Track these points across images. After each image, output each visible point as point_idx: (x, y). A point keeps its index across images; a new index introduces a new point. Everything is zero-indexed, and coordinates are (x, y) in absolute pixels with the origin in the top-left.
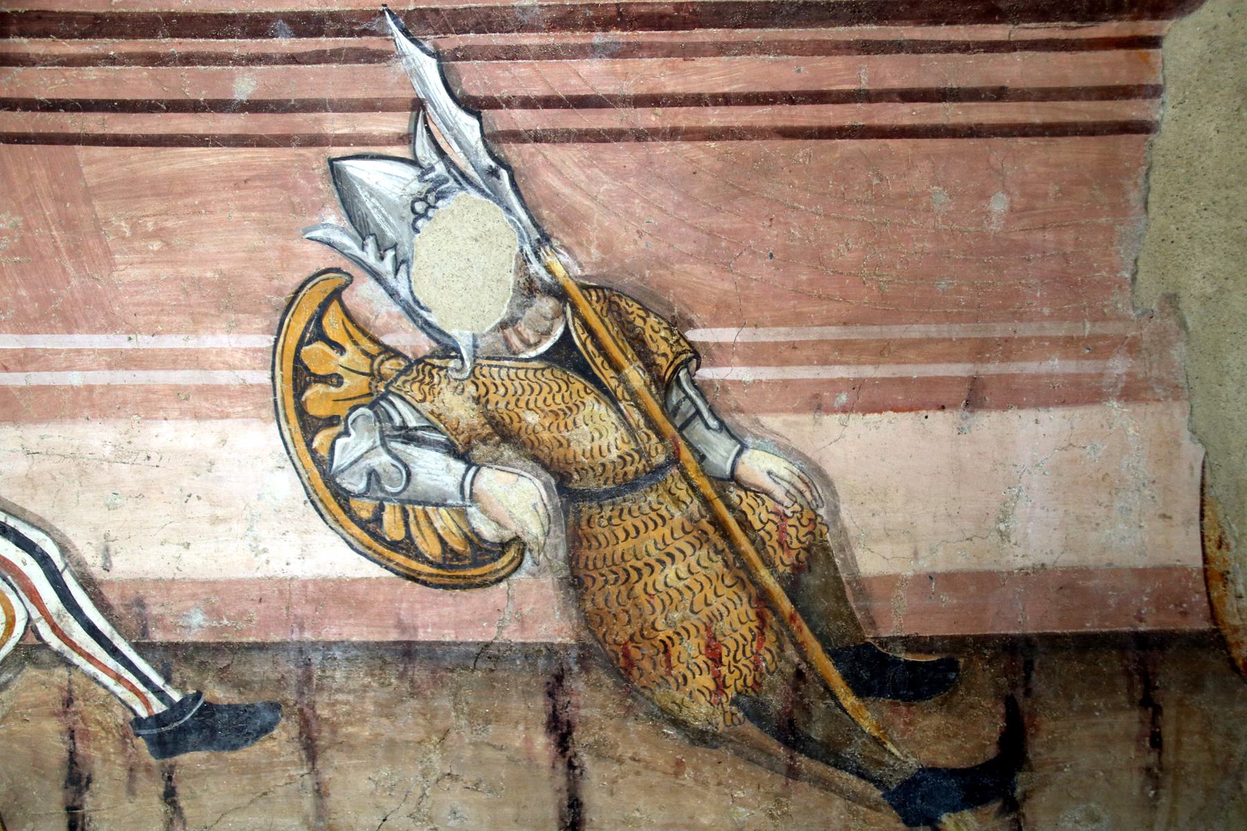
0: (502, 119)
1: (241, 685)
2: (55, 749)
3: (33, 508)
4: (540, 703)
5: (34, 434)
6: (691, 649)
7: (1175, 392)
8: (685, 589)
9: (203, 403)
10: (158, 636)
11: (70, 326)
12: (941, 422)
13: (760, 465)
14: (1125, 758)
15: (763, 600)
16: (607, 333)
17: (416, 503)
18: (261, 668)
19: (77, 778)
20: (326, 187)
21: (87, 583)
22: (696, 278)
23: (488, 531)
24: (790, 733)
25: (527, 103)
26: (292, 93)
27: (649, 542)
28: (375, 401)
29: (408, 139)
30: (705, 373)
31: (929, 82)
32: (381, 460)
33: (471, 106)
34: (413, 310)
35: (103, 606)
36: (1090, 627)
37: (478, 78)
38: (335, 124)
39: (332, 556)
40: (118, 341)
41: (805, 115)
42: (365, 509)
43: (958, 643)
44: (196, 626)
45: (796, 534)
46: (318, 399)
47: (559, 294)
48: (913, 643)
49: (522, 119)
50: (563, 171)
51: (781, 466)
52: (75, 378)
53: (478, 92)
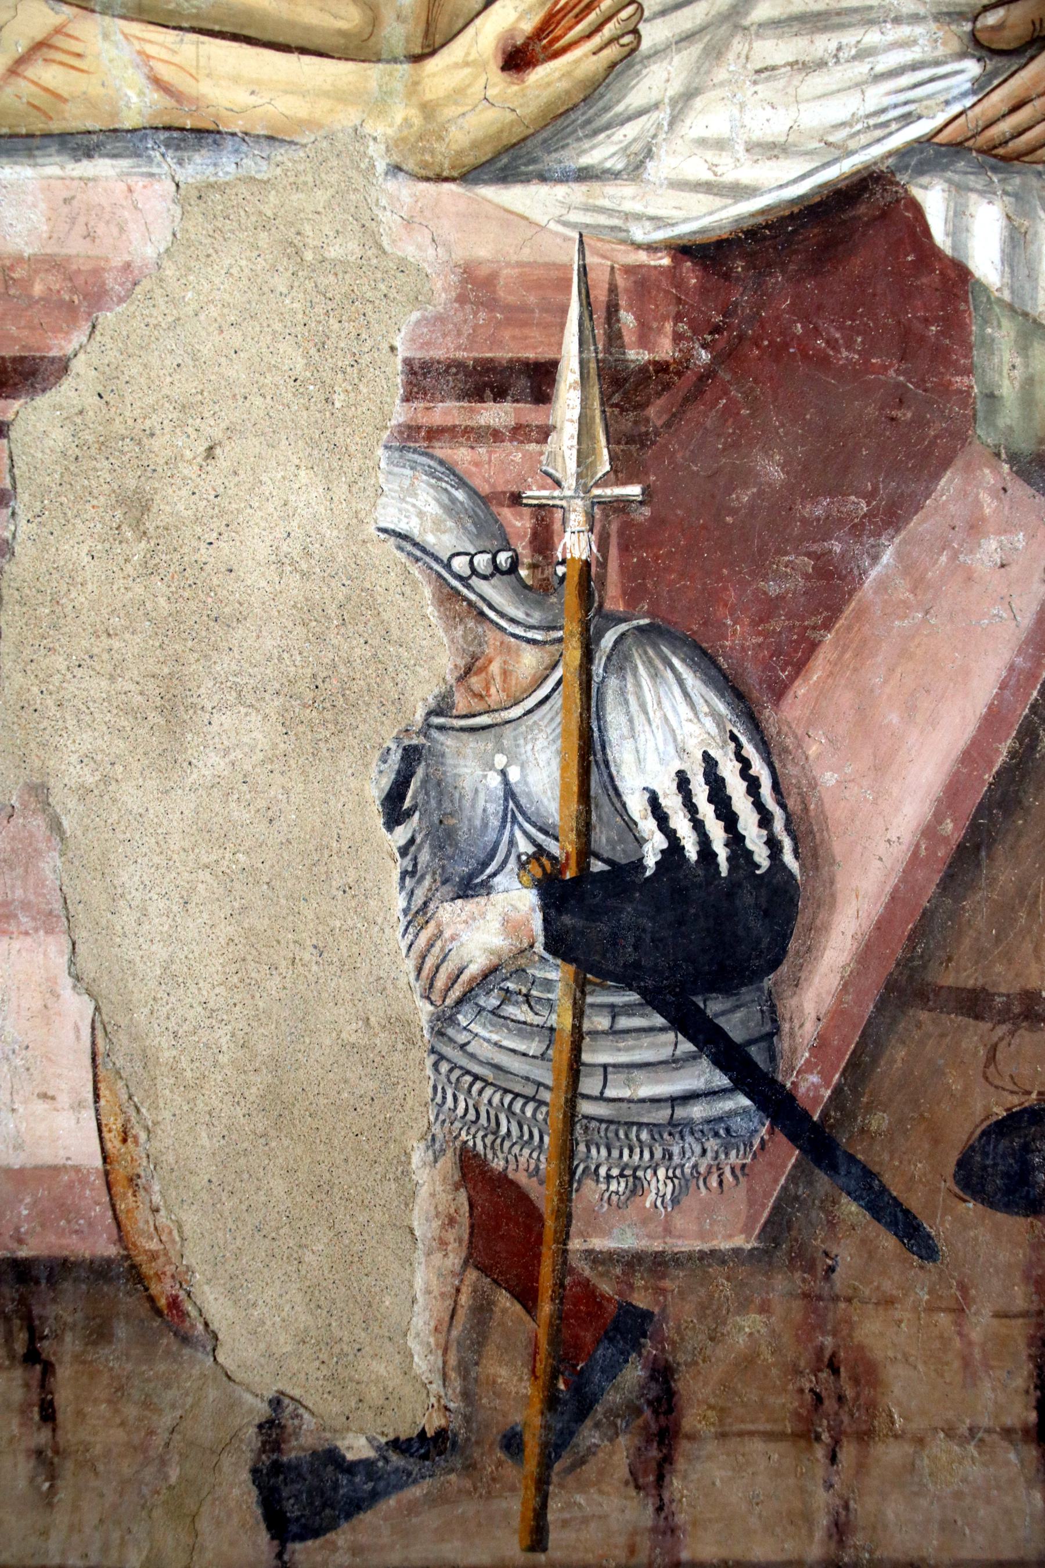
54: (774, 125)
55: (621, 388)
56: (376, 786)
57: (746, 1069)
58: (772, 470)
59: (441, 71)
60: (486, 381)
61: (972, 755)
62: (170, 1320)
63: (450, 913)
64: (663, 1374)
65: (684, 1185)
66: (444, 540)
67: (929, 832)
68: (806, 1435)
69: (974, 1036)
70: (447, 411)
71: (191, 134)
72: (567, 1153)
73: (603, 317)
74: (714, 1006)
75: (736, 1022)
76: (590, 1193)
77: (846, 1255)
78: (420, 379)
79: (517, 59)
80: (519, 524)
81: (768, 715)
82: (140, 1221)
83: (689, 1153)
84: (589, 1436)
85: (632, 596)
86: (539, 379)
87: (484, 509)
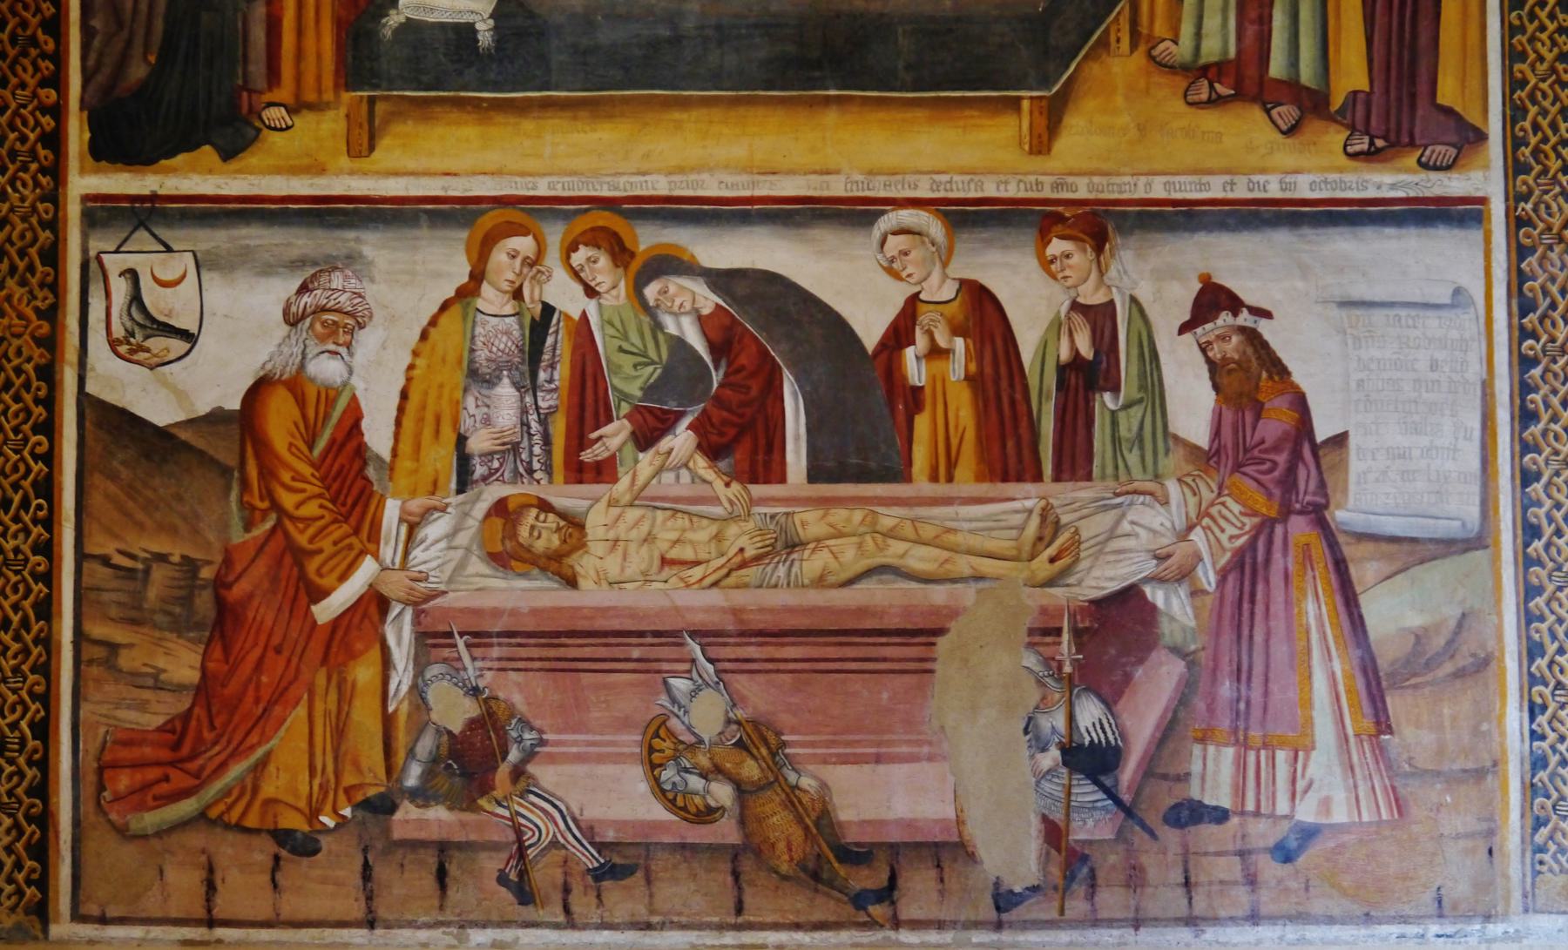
0: (721, 666)
1: (625, 857)
2: (560, 879)
3: (559, 793)
4: (729, 866)
5: (560, 768)
6: (782, 846)
7: (944, 758)
8: (779, 823)
9: (618, 759)
10: (598, 839)
11: (574, 732)
12: (866, 768)
13: (806, 782)
14: (933, 885)
15: (806, 828)
16: (756, 736)
17: (688, 793)
18: (632, 851)
19: (567, 890)
20: (662, 687)
21: (575, 820)
22: (785, 719)
23: (713, 804)
24: (816, 876)
25: (729, 660)
26: (652, 656)
27: (768, 809)
28: (675, 758)
29: (689, 671)
30: (787, 751)
31: (861, 655)
32: (677, 779)
33: (710, 661)
34: (689, 728)
35: (579, 827)
36: (919, 839)
37: (715, 652)
38: (665, 666)
39: (659, 813)
40: (590, 737)
41: (822, 666)
42: (670, 796)
43: (873, 844)
44: (610, 836)
45: (818, 806)
46: (656, 757)
47: (739, 723)
48: (858, 844)
49: (728, 665)
50: (741, 683)
51: (813, 783)
52: (574, 750)
53: (713, 656)
54: (1110, 573)
55: (1077, 633)
56: (1023, 725)
57: (1111, 794)
58: (1113, 651)
59: (1035, 563)
60: (1046, 632)
61: (1163, 717)
62: (972, 857)
63: (1039, 756)
64: (1092, 870)
65: (1097, 822)
66: (1037, 668)
67: (1153, 736)
68: (1128, 886)
69: (1165, 785)
70: (1037, 639)
71: (979, 578)
72: (1068, 815)
73: (1072, 616)
74: (1102, 778)
75: (1108, 782)
76: (1074, 825)
77: (1136, 840)
78: (1031, 632)
79: (1052, 560)
80: (1054, 664)
81: (1114, 709)
82: (965, 833)
83: (1097, 814)
84: (1075, 886)
85: (1082, 678)
86: (1058, 632)
87: (1047, 661)
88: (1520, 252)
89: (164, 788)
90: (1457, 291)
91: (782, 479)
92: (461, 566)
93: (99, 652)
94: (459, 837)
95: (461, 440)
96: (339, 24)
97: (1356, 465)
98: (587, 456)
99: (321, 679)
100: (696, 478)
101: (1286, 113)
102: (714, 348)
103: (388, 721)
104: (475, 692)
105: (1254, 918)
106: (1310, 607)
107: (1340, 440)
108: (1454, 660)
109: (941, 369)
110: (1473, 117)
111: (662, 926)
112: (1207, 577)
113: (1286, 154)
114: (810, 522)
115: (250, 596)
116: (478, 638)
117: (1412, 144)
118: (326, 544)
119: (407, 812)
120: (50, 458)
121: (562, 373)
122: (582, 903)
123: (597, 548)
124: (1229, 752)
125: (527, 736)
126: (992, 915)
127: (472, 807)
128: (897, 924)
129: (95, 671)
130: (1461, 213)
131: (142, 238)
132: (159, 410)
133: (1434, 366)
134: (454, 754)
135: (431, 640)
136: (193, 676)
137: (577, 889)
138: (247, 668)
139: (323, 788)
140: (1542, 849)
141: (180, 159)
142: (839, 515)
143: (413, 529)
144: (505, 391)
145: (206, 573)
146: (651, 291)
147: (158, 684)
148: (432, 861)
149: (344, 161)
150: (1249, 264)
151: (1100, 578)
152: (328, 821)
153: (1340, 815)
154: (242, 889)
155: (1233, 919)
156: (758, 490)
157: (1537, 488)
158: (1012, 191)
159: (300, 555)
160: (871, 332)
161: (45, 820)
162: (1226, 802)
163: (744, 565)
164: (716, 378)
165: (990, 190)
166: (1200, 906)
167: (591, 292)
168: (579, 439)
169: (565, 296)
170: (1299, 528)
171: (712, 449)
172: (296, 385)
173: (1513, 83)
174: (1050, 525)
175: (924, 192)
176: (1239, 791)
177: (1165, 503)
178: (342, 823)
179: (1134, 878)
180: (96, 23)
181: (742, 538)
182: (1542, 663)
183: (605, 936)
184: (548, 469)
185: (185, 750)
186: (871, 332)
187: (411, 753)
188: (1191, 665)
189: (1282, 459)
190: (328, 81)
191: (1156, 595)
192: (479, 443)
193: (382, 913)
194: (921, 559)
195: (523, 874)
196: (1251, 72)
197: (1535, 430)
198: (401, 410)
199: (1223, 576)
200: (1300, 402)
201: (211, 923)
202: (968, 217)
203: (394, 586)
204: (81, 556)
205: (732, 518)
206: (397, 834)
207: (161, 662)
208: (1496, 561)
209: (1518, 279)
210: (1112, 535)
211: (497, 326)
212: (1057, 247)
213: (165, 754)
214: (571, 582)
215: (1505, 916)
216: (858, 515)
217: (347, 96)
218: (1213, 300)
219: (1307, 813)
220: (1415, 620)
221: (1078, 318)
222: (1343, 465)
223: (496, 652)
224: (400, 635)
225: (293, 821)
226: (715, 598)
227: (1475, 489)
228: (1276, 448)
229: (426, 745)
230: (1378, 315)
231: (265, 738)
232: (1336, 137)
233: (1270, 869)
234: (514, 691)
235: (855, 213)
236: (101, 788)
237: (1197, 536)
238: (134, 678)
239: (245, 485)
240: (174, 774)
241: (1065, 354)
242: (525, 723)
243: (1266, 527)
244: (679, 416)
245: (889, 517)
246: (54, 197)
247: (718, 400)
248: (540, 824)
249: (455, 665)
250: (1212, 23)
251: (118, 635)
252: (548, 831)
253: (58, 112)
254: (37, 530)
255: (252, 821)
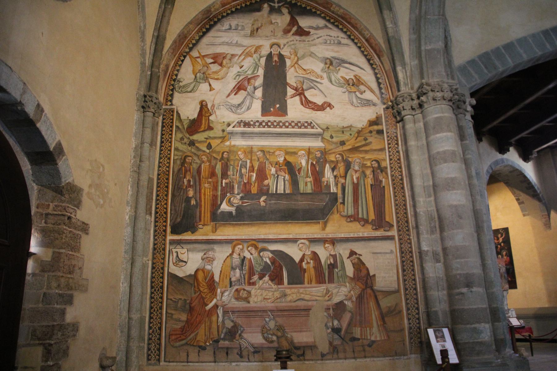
13: (289, 336)
16: (280, 328)
19: (248, 355)
28: (267, 332)
37: (273, 314)
39: (264, 342)
44: (256, 346)
50: (277, 319)
55: (333, 309)
57: (340, 336)
62: (317, 348)
71: (316, 300)
78: (326, 309)
86: (330, 309)
87: (328, 314)
88: (401, 244)
89: (180, 339)
90: (392, 251)
91: (283, 284)
92: (231, 299)
93: (170, 315)
94: (230, 346)
95: (230, 279)
96: (211, 211)
97: (377, 279)
98: (251, 281)
99: (207, 320)
100: (269, 284)
101: (362, 223)
102: (272, 263)
103: (218, 326)
104: (233, 321)
105: (365, 357)
106: (371, 303)
107: (374, 275)
108: (394, 311)
109: (309, 266)
110: (391, 223)
111: (265, 361)
112: (354, 299)
113: (362, 229)
114: (288, 291)
115: (195, 305)
116: (233, 312)
117: (382, 227)
118: (208, 297)
119: (221, 342)
120: (162, 283)
121: (247, 267)
122: (251, 358)
123: (253, 297)
124: (359, 328)
125: (242, 329)
126: (320, 358)
127: (233, 341)
128: (305, 360)
129: (169, 318)
130: (391, 238)
131: (178, 246)
132: (181, 274)
133: (389, 263)
134: (230, 332)
135: (225, 312)
136: (186, 319)
137: (250, 356)
138: (195, 318)
139: (207, 339)
140: (412, 343)
141: (185, 233)
142: (293, 290)
143: (222, 293)
144: (238, 270)
145: (188, 302)
146: (261, 254)
147: (179, 320)
148: (226, 351)
149: (211, 234)
150: (358, 248)
151: (336, 300)
152: (208, 344)
153: (378, 339)
154: (193, 356)
155: (361, 358)
156: (280, 286)
157: (407, 282)
158: (319, 236)
159: (203, 299)
160: (297, 259)
161: (160, 344)
162: (359, 337)
163: (277, 299)
164: (272, 268)
165: (316, 237)
166: (356, 355)
167: (251, 254)
168: (250, 278)
169: (247, 255)
170: (369, 291)
171: (272, 280)
172: (203, 270)
173: (397, 217)
174: (328, 291)
175: (305, 237)
176: (361, 335)
177: (346, 286)
178: (210, 344)
179: (345, 351)
180: (172, 212)
181: (277, 294)
182: (410, 311)
183: (255, 363)
184: (245, 283)
185: (184, 332)
186: (297, 259)
187: (222, 332)
188: (352, 314)
189: (365, 279)
190: (209, 221)
191: (346, 302)
192: (233, 279)
193: (217, 360)
194: (307, 297)
195: (241, 353)
196: (356, 216)
197: (405, 273)
198: (220, 274)
199: (356, 299)
200: (367, 269)
201: (188, 362)
202: (313, 241)
203: (219, 303)
204: (167, 299)
205: (275, 291)
206: (219, 346)
207: (180, 317)
208: (401, 295)
209: (401, 248)
210: (338, 292)
211: (236, 259)
212: (327, 245)
213: (180, 333)
214: (249, 302)
215: (407, 355)
216: (296, 290)
217: (212, 223)
218: (352, 253)
219: (373, 338)
220: (389, 305)
221: (331, 257)
222: (375, 280)
223: (236, 314)
224: (220, 312)
225: (202, 344)
226: (273, 305)
227: (396, 283)
228: (364, 277)
229: (224, 331)
230: (379, 255)
231: (197, 329)
232: (370, 227)
233: (367, 348)
234: (239, 321)
235: (294, 241)
236: (169, 338)
237: (352, 292)
238: (176, 320)
239: (195, 287)
240: (182, 336)
241: (329, 263)
242: (241, 327)
243: (363, 290)
244: (266, 274)
245: (301, 290)
246: (165, 240)
247: (273, 272)
248: (244, 344)
249: (229, 318)
250: (350, 209)
251: (173, 312)
252: (245, 345)
253: (166, 226)
254: (160, 295)
255: (195, 344)
